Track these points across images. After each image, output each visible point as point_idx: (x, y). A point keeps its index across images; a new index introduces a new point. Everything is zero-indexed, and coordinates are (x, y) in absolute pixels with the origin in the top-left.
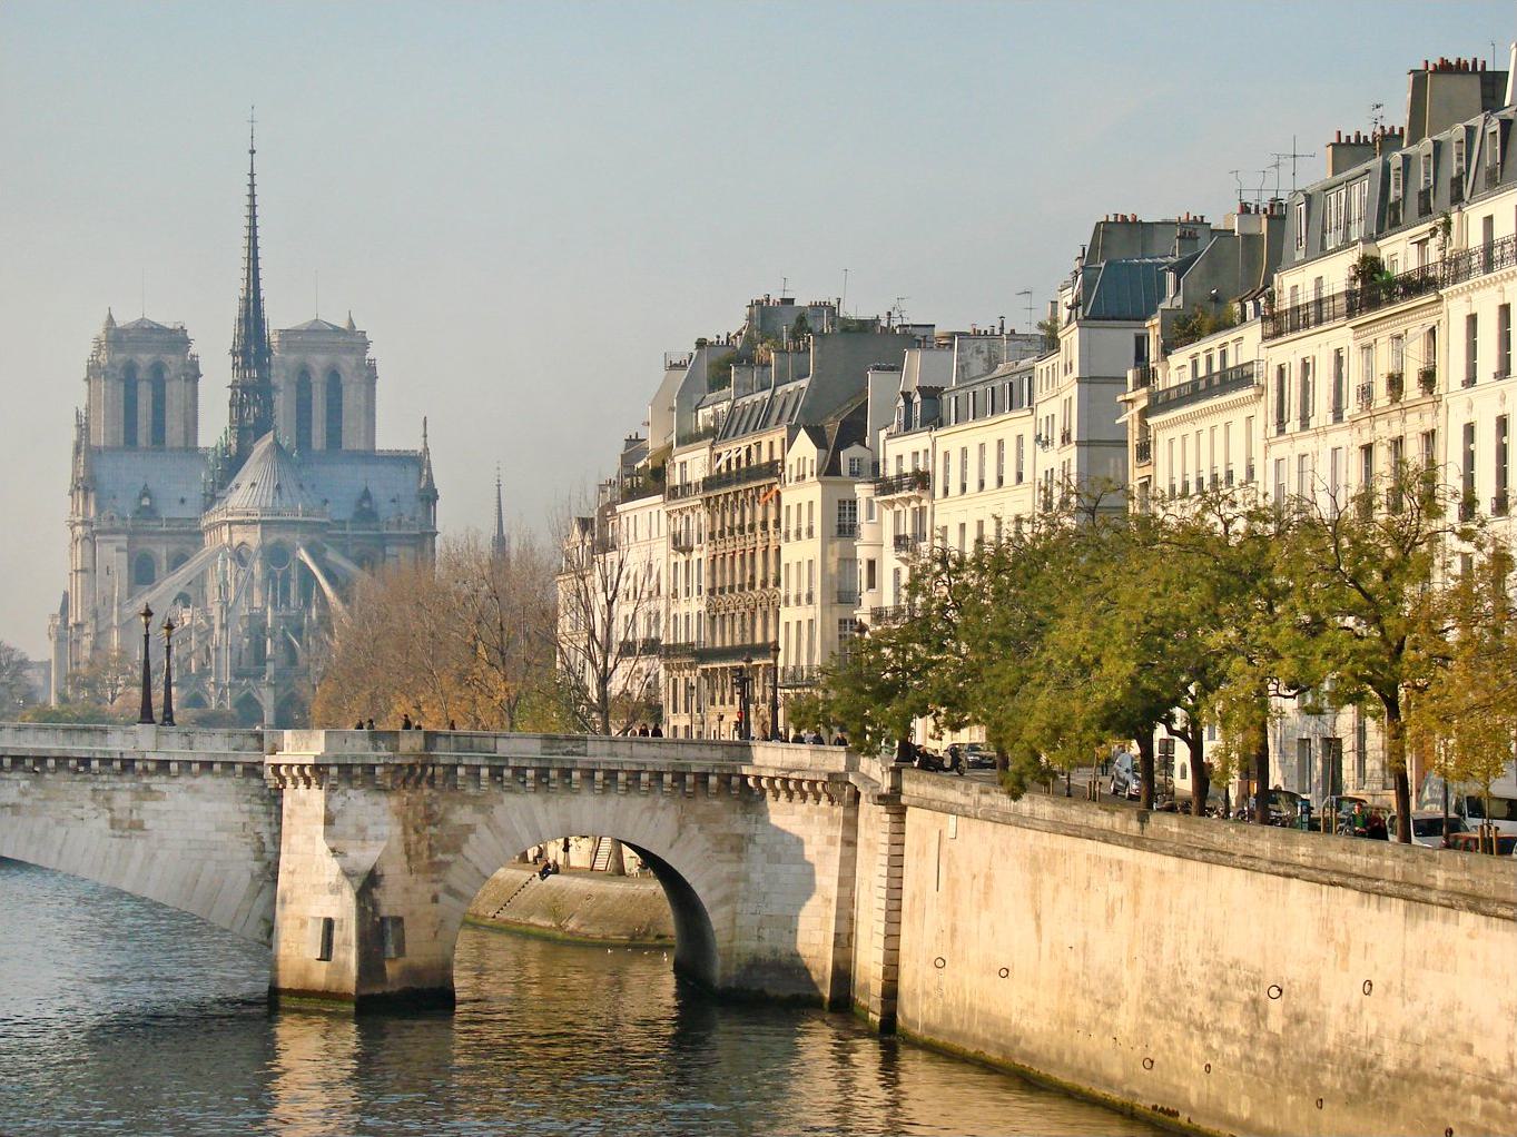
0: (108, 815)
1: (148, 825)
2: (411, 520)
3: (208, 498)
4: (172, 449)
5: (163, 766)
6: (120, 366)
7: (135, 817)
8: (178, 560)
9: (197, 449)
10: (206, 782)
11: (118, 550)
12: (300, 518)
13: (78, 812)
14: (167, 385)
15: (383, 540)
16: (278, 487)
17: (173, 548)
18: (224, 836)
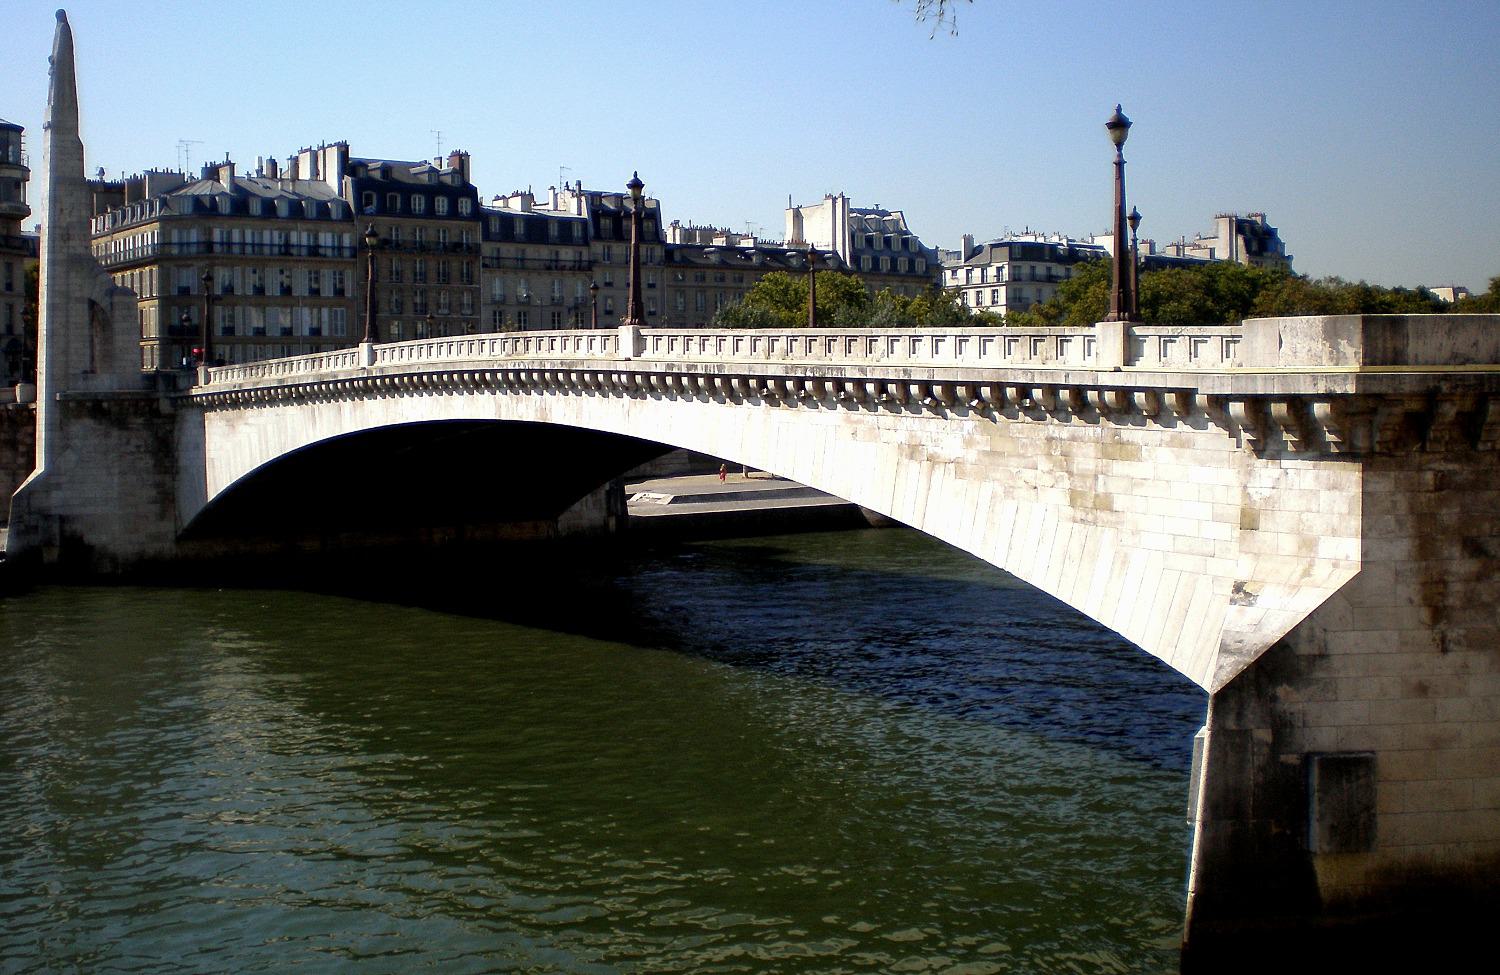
0: (1066, 484)
1: (1119, 503)
7: (1101, 489)
13: (1028, 474)
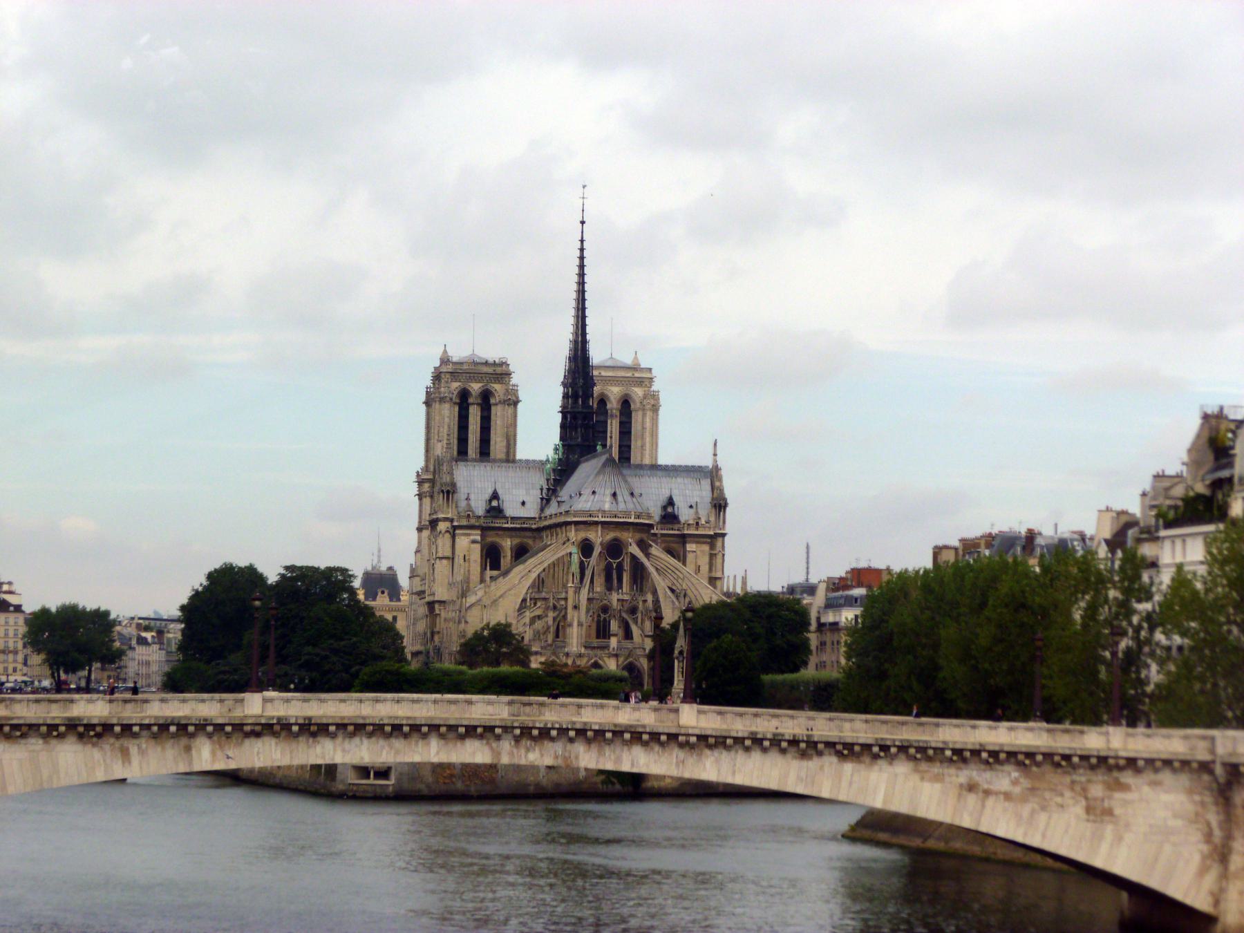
1: (1117, 811)
2: (706, 523)
3: (544, 501)
4: (501, 461)
5: (1131, 763)
6: (455, 393)
7: (1106, 804)
8: (521, 553)
9: (514, 461)
10: (1166, 776)
11: (474, 542)
12: (632, 520)
13: (1059, 800)
14: (493, 408)
15: (683, 539)
16: (614, 495)
17: (517, 541)
18: (1179, 823)
